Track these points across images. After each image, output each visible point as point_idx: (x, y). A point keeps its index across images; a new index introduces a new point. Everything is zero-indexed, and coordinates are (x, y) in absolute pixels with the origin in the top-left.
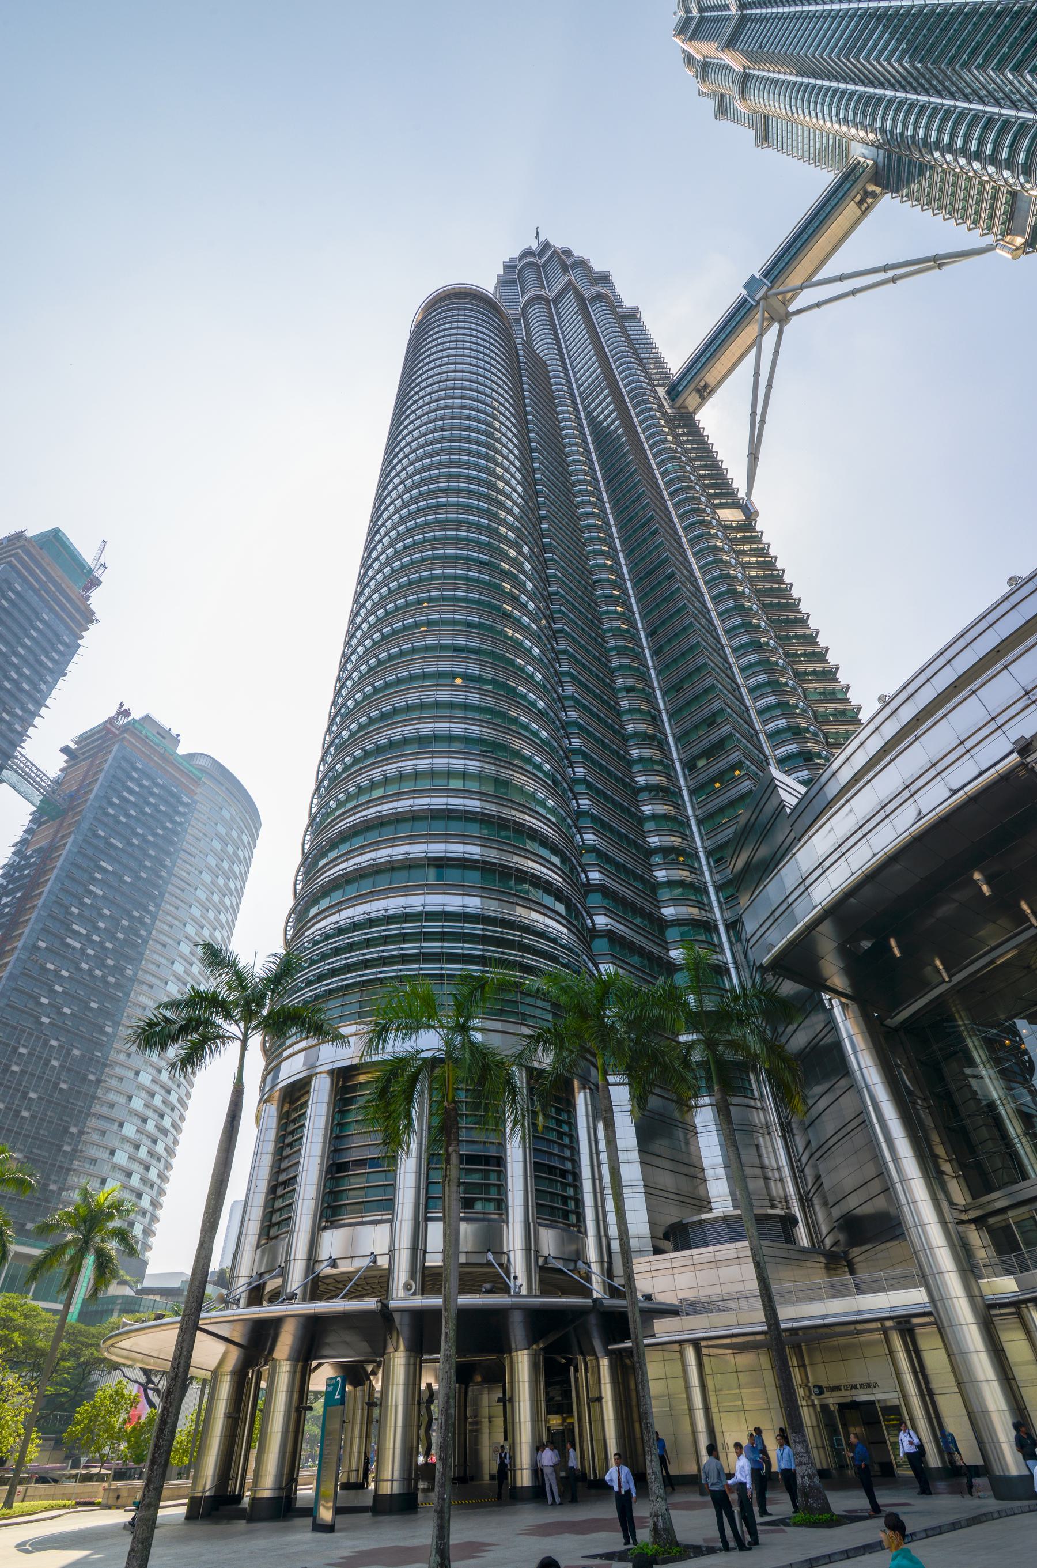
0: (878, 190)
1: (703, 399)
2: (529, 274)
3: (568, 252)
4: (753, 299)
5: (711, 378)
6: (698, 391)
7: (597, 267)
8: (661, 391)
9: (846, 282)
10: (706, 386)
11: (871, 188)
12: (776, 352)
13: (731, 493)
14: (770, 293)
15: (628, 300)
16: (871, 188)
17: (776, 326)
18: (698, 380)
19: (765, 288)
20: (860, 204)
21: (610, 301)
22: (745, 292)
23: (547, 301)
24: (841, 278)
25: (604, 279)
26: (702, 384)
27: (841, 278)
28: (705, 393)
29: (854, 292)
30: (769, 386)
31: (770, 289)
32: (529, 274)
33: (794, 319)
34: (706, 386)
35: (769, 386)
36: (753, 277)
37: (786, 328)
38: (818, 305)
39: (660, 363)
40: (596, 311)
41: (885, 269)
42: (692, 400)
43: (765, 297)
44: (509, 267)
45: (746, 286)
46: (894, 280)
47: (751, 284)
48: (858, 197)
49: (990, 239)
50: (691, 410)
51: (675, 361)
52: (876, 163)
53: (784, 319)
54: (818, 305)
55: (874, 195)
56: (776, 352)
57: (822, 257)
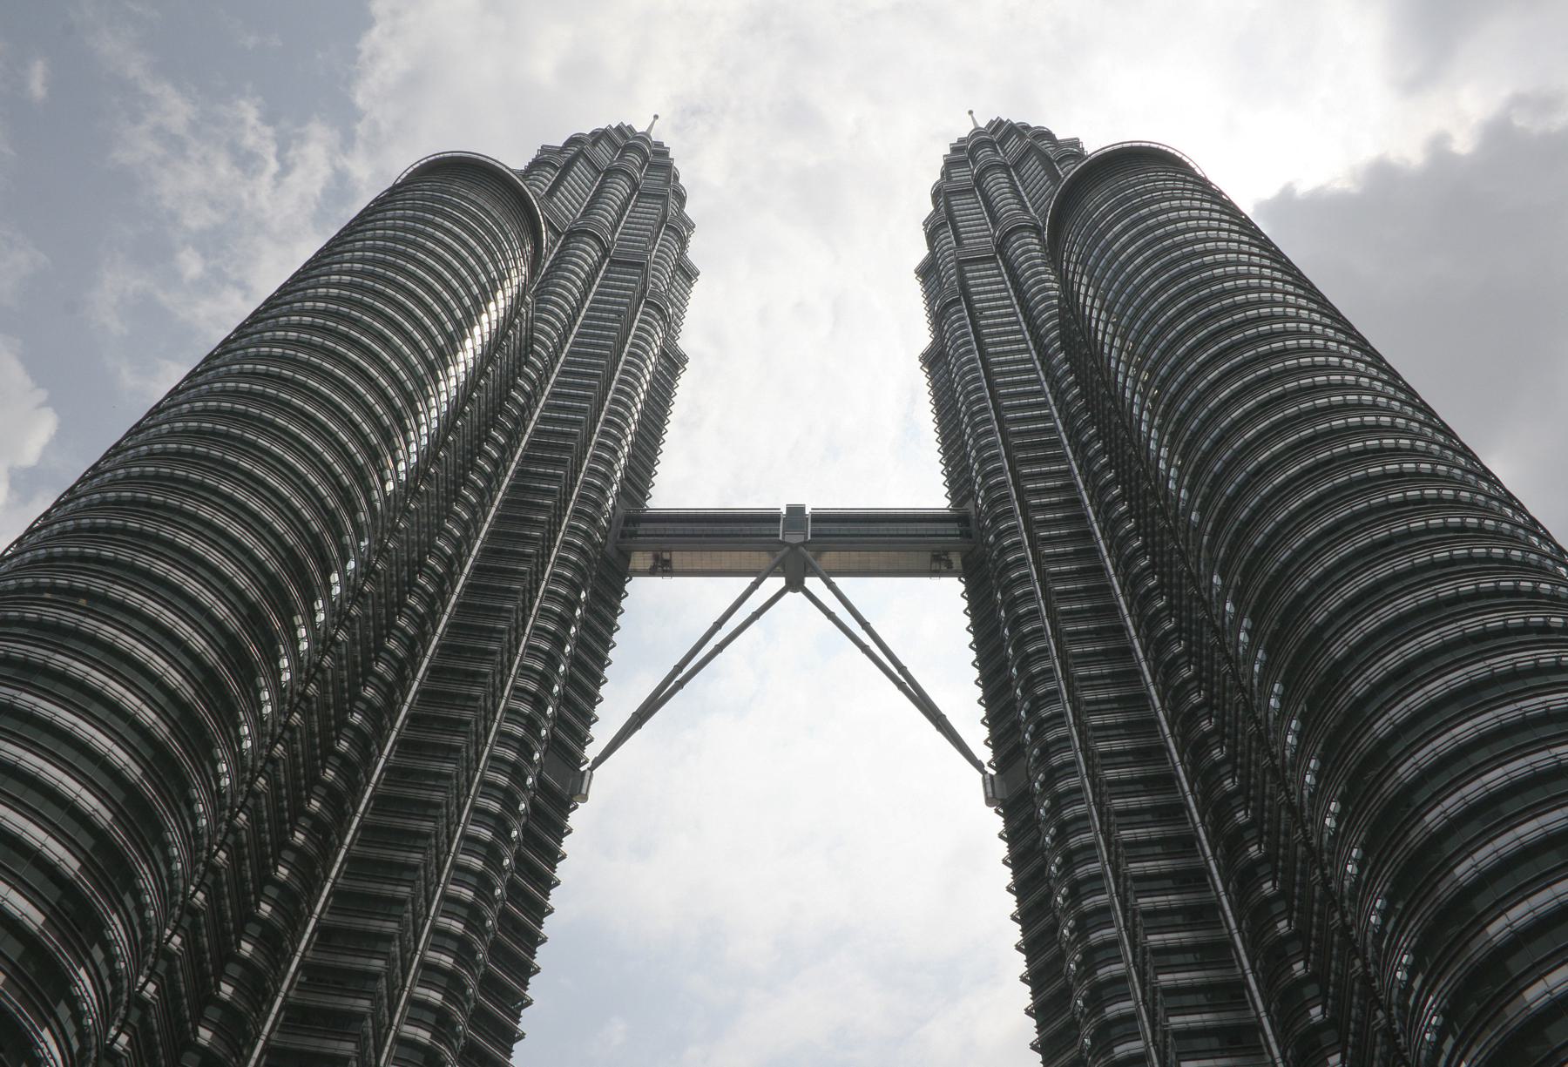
1: (652, 572)
4: (784, 535)
5: (678, 559)
6: (656, 558)
12: (756, 615)
15: (687, 341)
18: (666, 546)
19: (800, 539)
20: (936, 558)
26: (666, 556)
28: (662, 568)
30: (719, 648)
31: (804, 544)
33: (800, 594)
34: (668, 562)
39: (644, 494)
43: (794, 547)
46: (900, 686)
47: (796, 511)
53: (795, 585)
54: (830, 615)
55: (949, 564)
56: (756, 615)
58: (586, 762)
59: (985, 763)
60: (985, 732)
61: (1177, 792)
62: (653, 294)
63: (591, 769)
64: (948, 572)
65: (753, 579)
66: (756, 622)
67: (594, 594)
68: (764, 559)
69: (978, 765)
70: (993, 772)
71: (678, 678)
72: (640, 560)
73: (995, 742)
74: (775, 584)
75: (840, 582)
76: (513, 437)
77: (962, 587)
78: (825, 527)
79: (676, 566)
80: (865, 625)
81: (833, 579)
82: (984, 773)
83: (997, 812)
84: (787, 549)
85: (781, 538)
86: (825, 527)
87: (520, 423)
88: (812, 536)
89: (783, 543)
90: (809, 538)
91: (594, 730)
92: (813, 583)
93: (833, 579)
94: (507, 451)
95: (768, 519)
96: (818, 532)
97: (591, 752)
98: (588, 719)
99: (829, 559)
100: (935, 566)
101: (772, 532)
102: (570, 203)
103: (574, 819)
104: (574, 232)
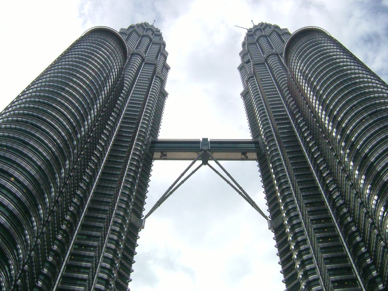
1: (161, 158)
4: (202, 147)
5: (169, 154)
8: (150, 140)
12: (194, 172)
13: (141, 209)
14: (208, 152)
18: (165, 151)
21: (163, 82)
22: (201, 140)
26: (165, 153)
28: (163, 157)
29: (228, 182)
31: (209, 150)
33: (207, 166)
35: (183, 182)
36: (206, 139)
37: (203, 166)
38: (217, 172)
40: (156, 82)
41: (241, 188)
42: (157, 154)
43: (205, 151)
45: (204, 139)
46: (240, 193)
47: (205, 140)
49: (268, 214)
51: (164, 134)
53: (205, 163)
54: (217, 172)
56: (194, 172)
57: (229, 157)
58: (143, 216)
59: (268, 216)
60: (267, 207)
61: (328, 214)
62: (158, 73)
63: (145, 219)
65: (191, 162)
66: (194, 174)
67: (144, 165)
68: (195, 155)
69: (266, 217)
70: (271, 219)
71: (170, 191)
73: (271, 210)
74: (199, 162)
75: (220, 162)
76: (119, 115)
77: (257, 164)
78: (214, 145)
80: (228, 175)
81: (218, 161)
82: (267, 219)
83: (272, 231)
84: (203, 151)
85: (201, 148)
86: (214, 145)
87: (121, 111)
88: (210, 147)
89: (202, 150)
90: (210, 148)
91: (145, 207)
92: (212, 163)
93: (218, 161)
94: (117, 119)
95: (197, 142)
96: (212, 147)
97: (145, 213)
98: (143, 203)
99: (215, 155)
102: (131, 46)
103: (140, 234)
104: (134, 54)
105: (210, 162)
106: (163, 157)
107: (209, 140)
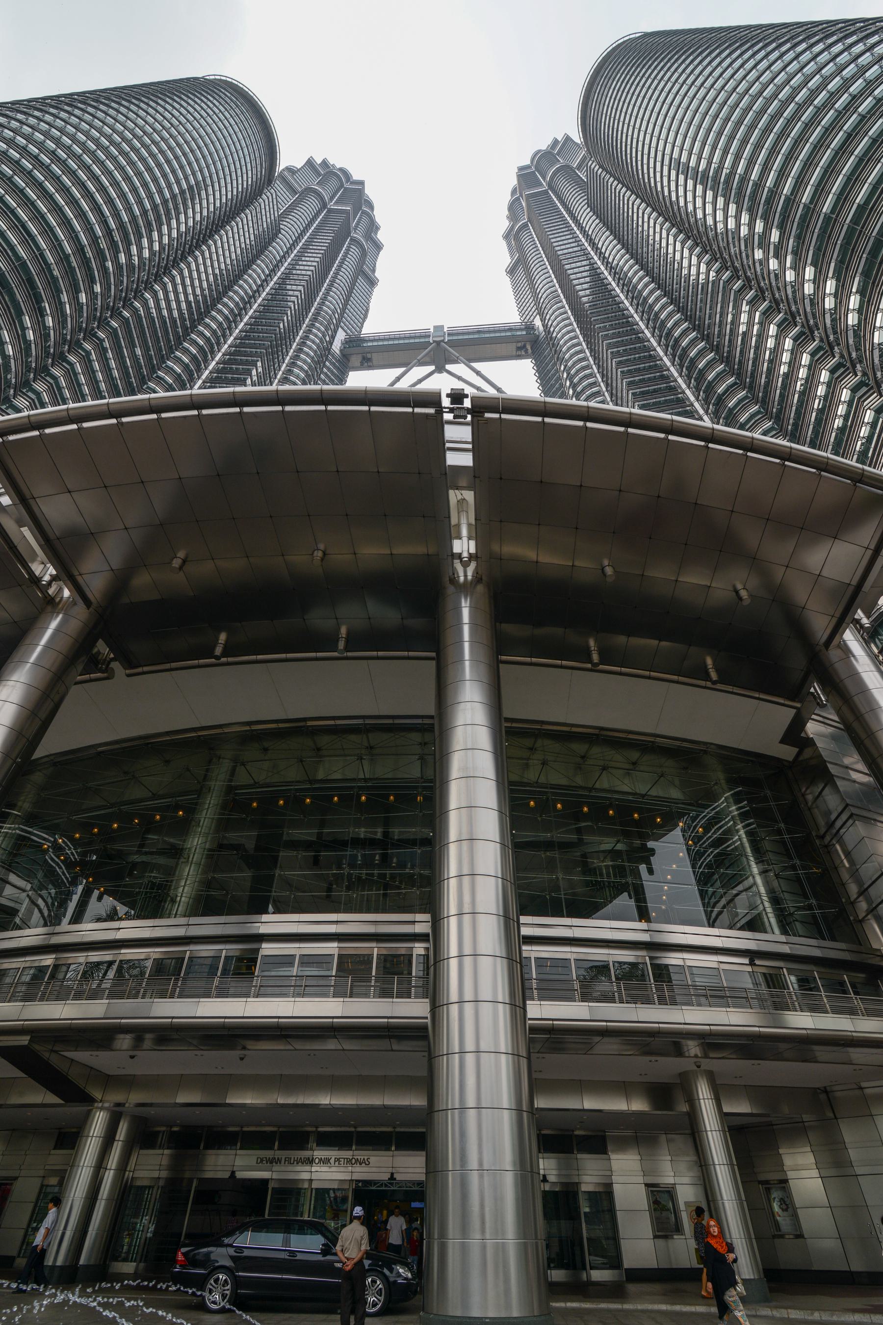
0: (530, 351)
2: (333, 183)
3: (371, 206)
6: (364, 358)
7: (381, 236)
8: (341, 335)
9: (479, 378)
10: (369, 360)
11: (529, 347)
16: (529, 347)
17: (433, 368)
19: (442, 338)
20: (519, 349)
22: (432, 330)
23: (324, 205)
24: (478, 373)
25: (378, 247)
26: (369, 356)
27: (478, 373)
31: (443, 341)
32: (333, 183)
33: (445, 374)
34: (369, 360)
37: (436, 375)
42: (355, 360)
43: (438, 343)
44: (325, 163)
45: (435, 327)
48: (519, 345)
50: (350, 364)
52: (538, 336)
53: (440, 369)
55: (526, 351)
64: (525, 357)
72: (355, 360)
79: (375, 362)
89: (434, 341)
100: (519, 353)
101: (427, 340)
105: (448, 367)
106: (366, 364)
107: (446, 330)
